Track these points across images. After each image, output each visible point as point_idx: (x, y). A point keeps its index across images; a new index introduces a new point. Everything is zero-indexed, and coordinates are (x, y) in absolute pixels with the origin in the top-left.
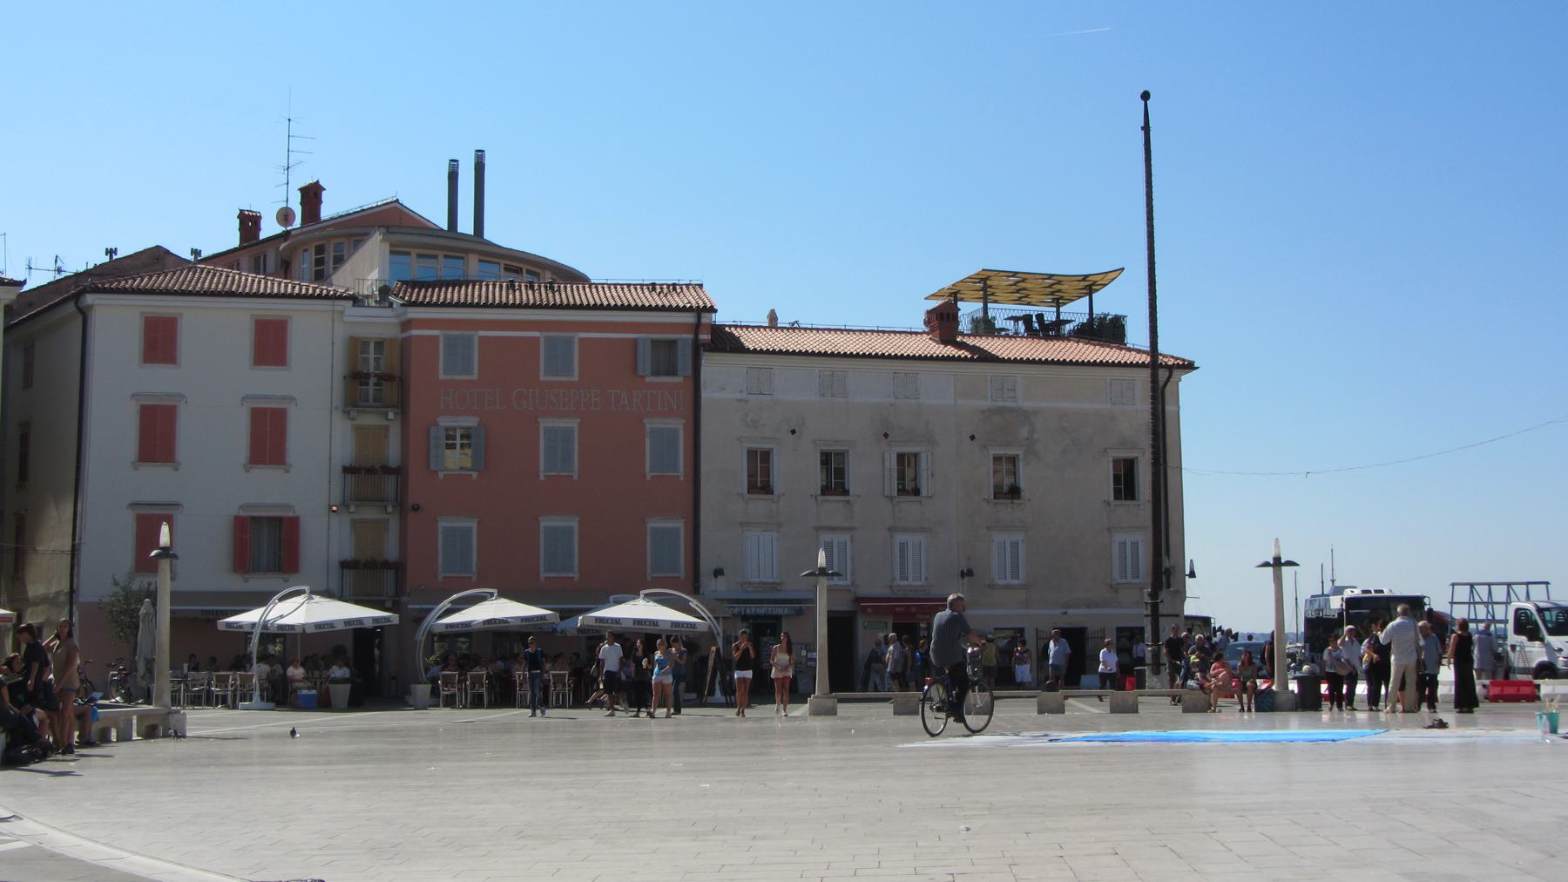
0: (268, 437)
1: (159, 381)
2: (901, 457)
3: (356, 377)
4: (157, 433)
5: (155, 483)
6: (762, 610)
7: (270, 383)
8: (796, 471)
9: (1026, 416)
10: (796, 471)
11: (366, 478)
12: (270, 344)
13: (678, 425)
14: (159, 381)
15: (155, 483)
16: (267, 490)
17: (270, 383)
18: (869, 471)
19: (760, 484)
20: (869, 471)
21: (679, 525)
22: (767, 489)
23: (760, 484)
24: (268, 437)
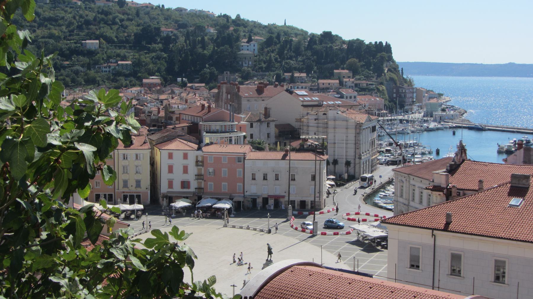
0: (185, 170)
1: (170, 162)
2: (276, 175)
3: (197, 162)
4: (171, 169)
5: (171, 176)
6: (253, 197)
7: (185, 162)
8: (259, 177)
9: (297, 168)
10: (259, 177)
11: (199, 176)
12: (185, 156)
13: (242, 170)
14: (170, 162)
15: (171, 176)
16: (185, 177)
17: (185, 162)
18: (271, 177)
19: (254, 179)
20: (271, 177)
21: (242, 184)
22: (255, 179)
23: (254, 179)
24: (185, 170)
